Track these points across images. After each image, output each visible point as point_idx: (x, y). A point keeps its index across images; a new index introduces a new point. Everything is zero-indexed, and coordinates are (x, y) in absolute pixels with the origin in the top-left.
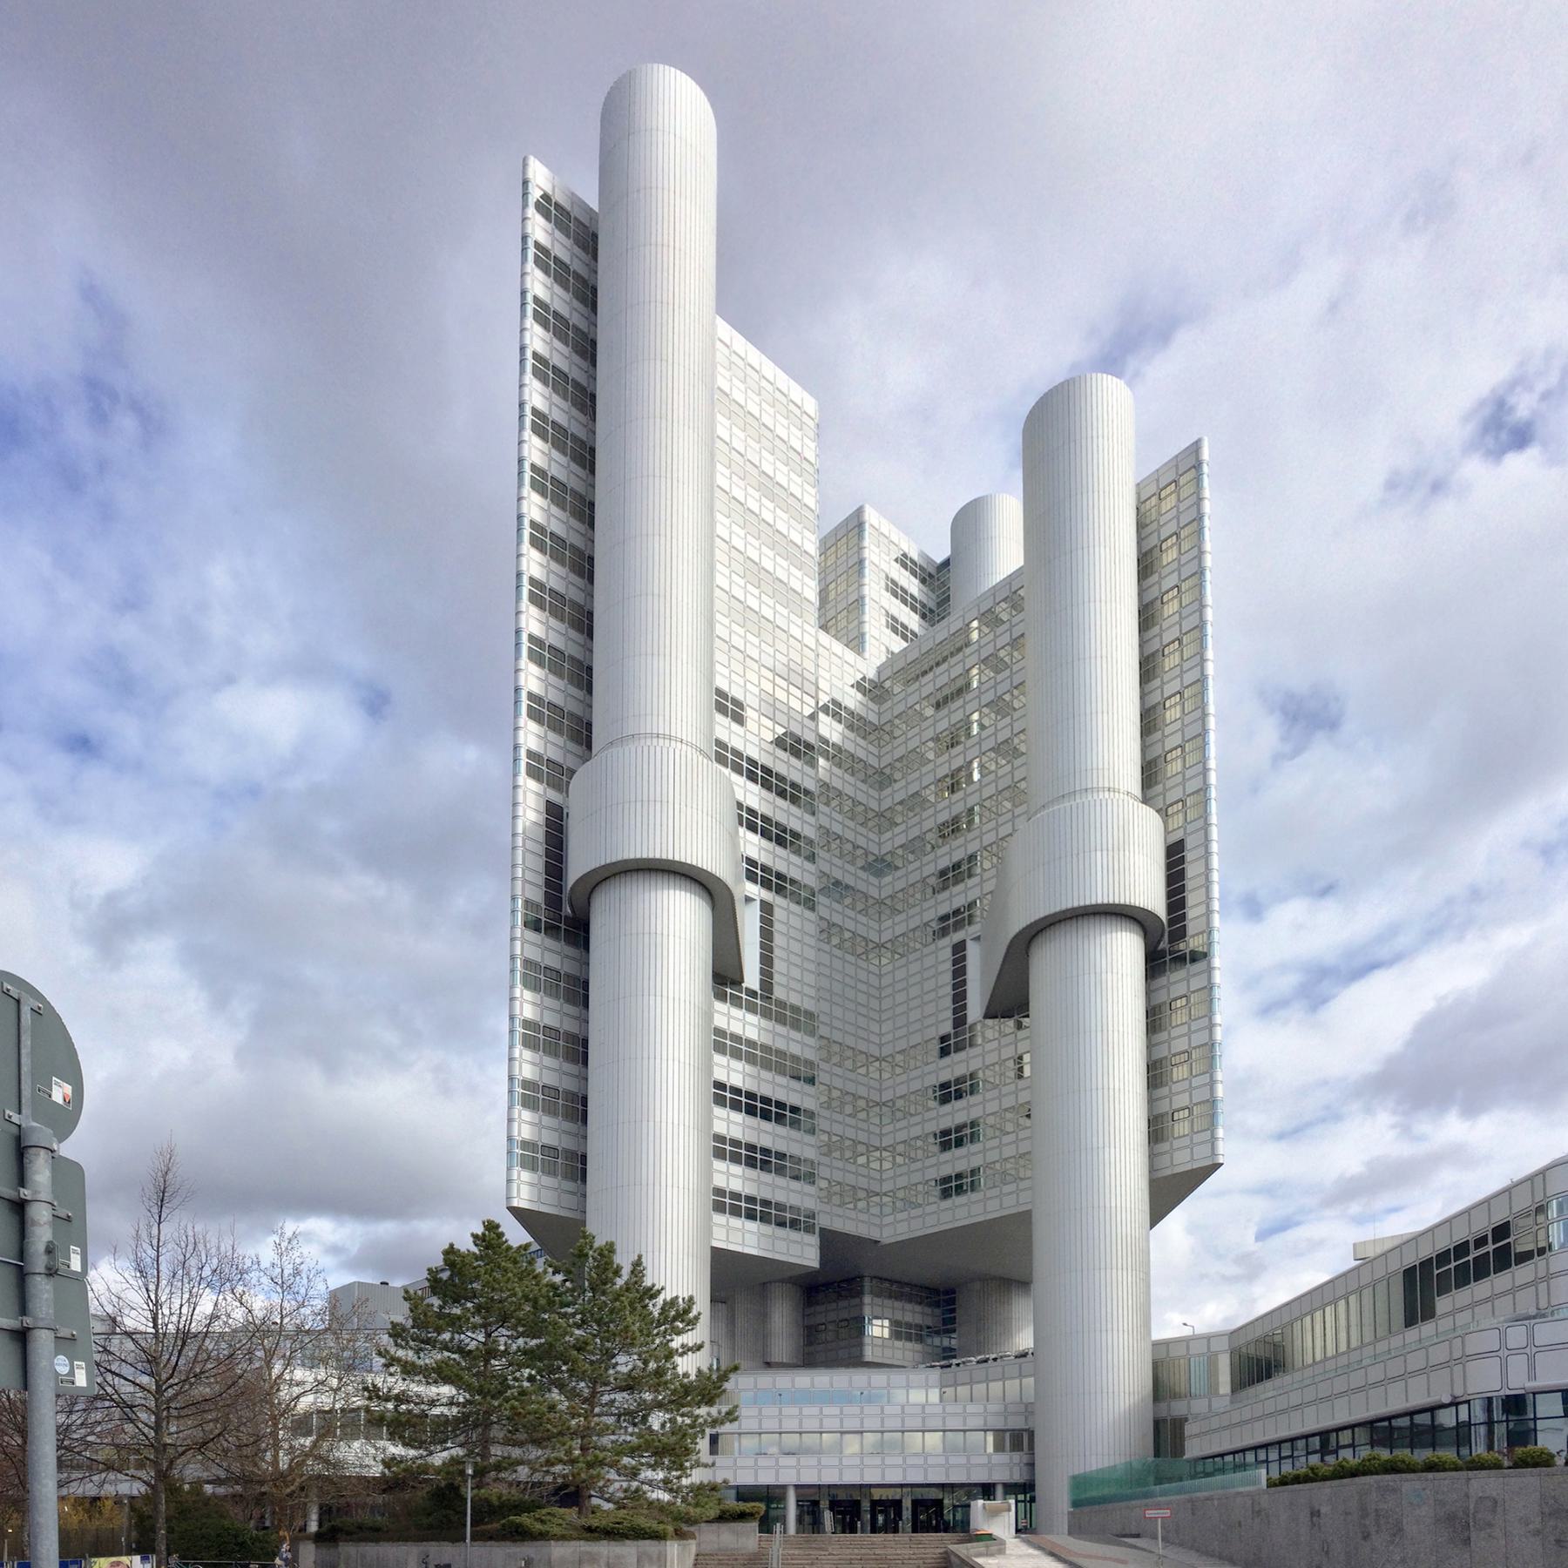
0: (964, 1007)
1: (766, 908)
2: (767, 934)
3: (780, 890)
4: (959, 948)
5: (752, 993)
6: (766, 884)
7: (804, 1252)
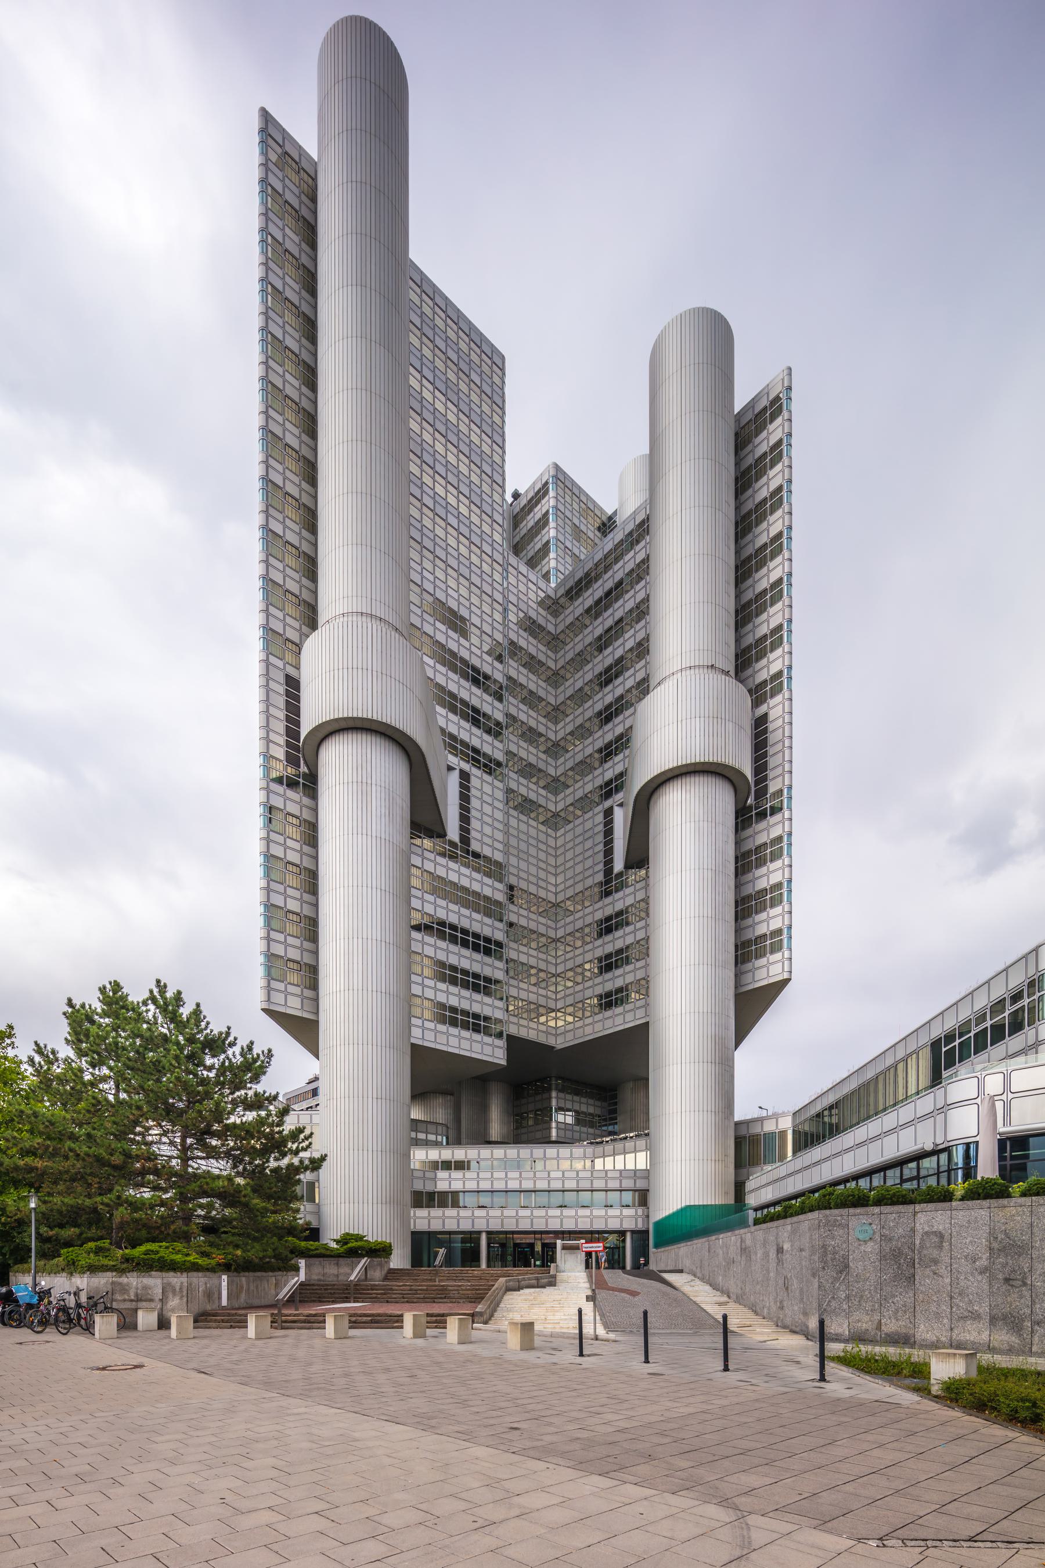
1: (465, 776)
2: (465, 798)
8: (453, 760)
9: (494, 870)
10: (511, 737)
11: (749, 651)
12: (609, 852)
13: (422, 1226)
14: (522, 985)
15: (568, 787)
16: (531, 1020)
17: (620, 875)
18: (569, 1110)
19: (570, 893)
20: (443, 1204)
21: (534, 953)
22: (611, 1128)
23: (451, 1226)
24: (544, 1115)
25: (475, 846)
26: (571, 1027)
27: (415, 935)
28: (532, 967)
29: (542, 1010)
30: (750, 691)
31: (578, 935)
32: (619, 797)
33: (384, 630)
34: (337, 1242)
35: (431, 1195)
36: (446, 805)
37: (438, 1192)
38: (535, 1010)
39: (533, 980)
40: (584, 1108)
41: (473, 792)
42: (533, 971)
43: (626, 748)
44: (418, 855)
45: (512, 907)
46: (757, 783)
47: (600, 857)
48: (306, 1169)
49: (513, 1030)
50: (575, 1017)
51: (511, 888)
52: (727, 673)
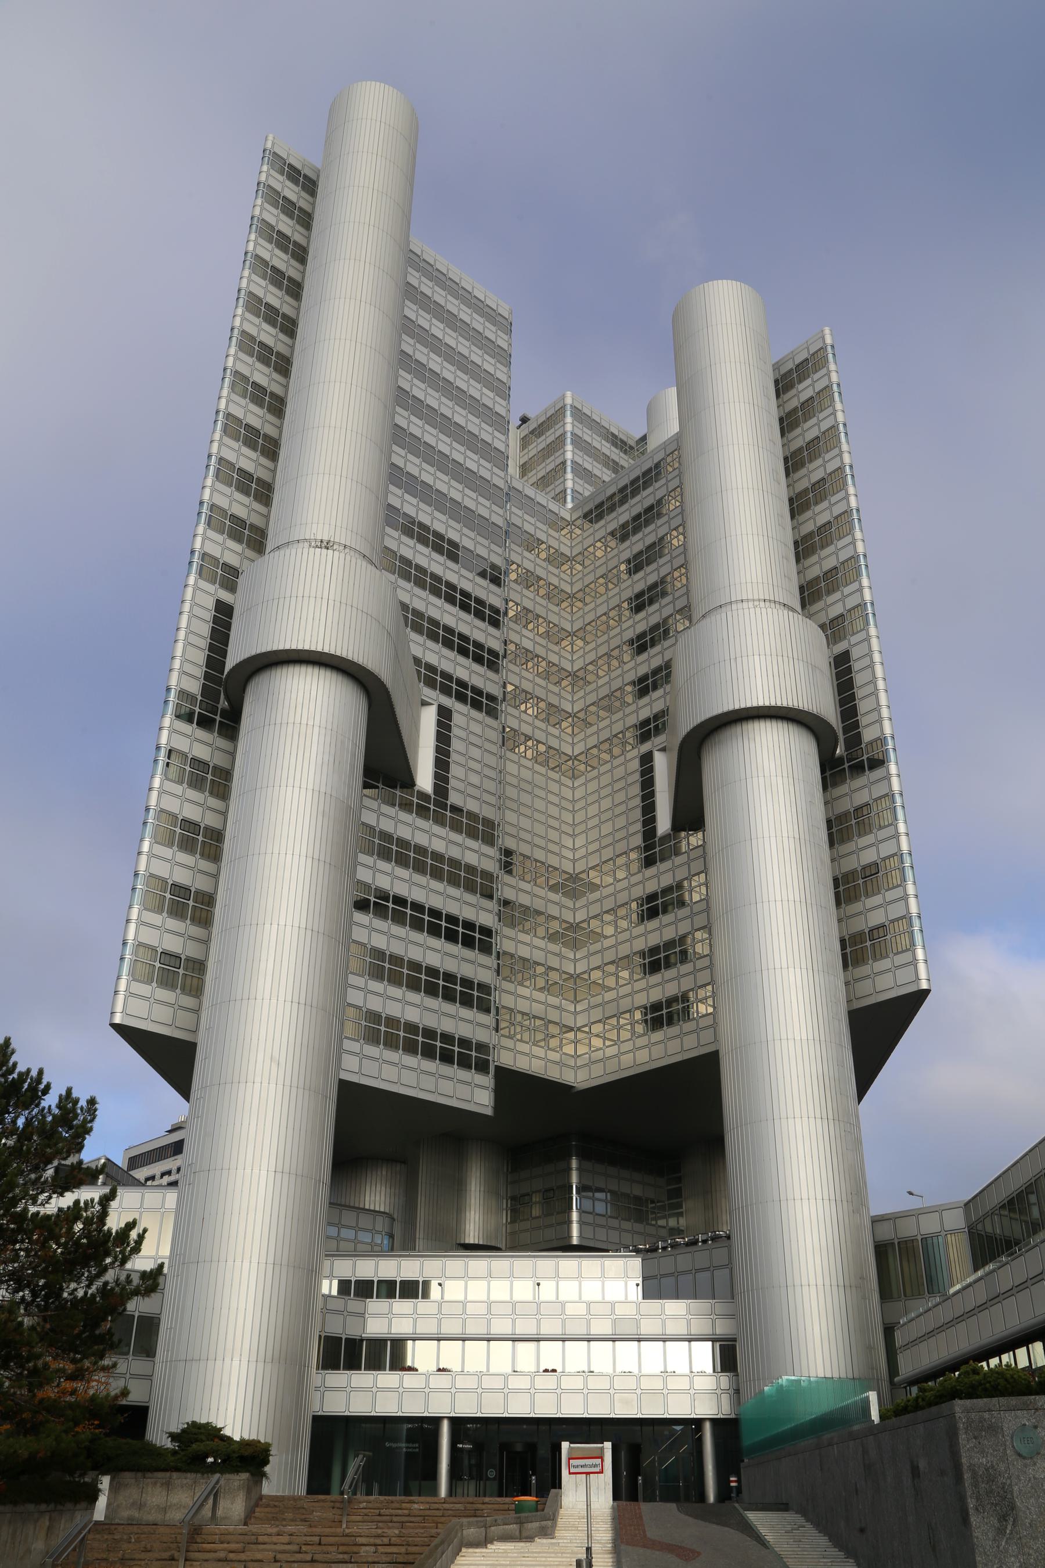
0: (653, 819)
1: (444, 714)
2: (443, 738)
3: (461, 698)
4: (647, 760)
5: (423, 796)
6: (446, 691)
7: (476, 1095)
8: (428, 693)
9: (482, 830)
10: (511, 667)
11: (819, 583)
12: (649, 808)
13: (336, 1405)
14: (521, 991)
15: (591, 725)
16: (536, 1043)
17: (666, 838)
18: (600, 1190)
19: (594, 860)
20: (375, 1364)
21: (541, 943)
22: (672, 1222)
23: (387, 1407)
24: (557, 1202)
25: (454, 798)
26: (599, 1055)
27: (360, 917)
28: (539, 964)
29: (553, 1029)
30: (822, 627)
31: (608, 918)
32: (659, 740)
33: (348, 557)
34: (173, 1437)
35: (354, 1345)
36: (416, 752)
37: (370, 1341)
38: (545, 1028)
39: (541, 982)
40: (625, 1188)
41: (455, 731)
42: (540, 970)
43: (668, 682)
45: (507, 879)
46: (846, 730)
47: (636, 790)
48: (136, 1292)
49: (505, 1059)
50: (605, 1039)
51: (508, 853)
52: (793, 610)
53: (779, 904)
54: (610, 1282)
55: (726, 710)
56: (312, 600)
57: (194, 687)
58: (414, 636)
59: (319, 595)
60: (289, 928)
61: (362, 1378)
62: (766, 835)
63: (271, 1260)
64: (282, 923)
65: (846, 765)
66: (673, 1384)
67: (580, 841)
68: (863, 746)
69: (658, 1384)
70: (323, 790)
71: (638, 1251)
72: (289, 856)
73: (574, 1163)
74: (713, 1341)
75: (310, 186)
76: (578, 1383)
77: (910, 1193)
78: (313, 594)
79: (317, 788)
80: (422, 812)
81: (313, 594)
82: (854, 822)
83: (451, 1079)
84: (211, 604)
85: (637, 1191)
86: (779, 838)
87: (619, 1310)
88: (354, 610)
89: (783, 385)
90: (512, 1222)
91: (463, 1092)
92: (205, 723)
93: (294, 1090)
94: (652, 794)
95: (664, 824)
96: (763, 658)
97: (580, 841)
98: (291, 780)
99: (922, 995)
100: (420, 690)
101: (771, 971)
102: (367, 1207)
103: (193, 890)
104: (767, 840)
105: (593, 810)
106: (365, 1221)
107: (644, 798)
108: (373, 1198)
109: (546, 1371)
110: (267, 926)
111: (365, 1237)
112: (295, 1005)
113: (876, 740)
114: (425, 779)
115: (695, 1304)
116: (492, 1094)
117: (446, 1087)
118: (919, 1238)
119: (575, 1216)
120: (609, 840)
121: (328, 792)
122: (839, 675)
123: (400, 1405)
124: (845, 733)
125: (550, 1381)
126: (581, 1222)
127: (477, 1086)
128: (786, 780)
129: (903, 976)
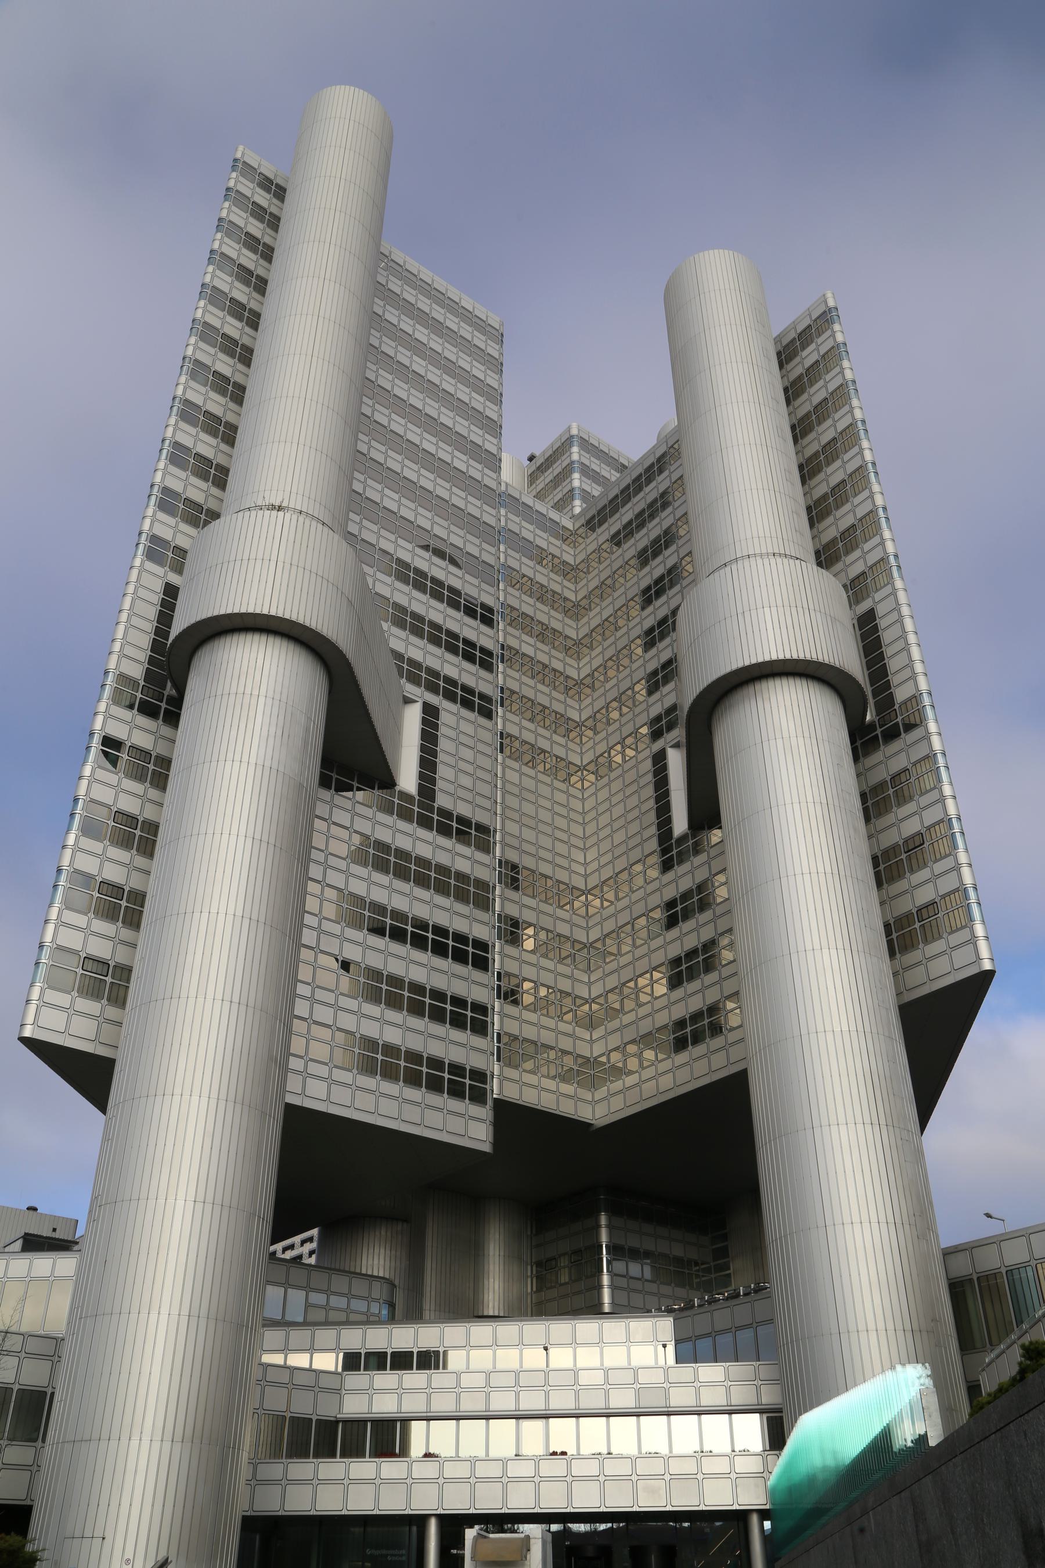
0: (669, 820)
1: (430, 713)
3: (450, 696)
4: (660, 759)
5: (405, 796)
6: (433, 688)
7: (470, 1128)
8: (411, 690)
25: (442, 801)
37: (345, 1422)
44: (346, 810)
53: (807, 877)
54: (635, 1346)
55: (734, 667)
56: (259, 562)
57: (137, 672)
58: (395, 630)
59: (267, 557)
60: (221, 916)
61: (332, 1468)
62: (788, 801)
63: (185, 1311)
64: (214, 910)
65: (879, 731)
66: (709, 1466)
67: (592, 854)
68: (897, 707)
69: (690, 1467)
70: (268, 764)
71: (669, 1311)
72: (225, 836)
73: (603, 1220)
74: (761, 1412)
75: (280, 193)
76: (592, 1468)
77: (988, 1216)
78: (260, 556)
79: (260, 762)
80: (405, 815)
81: (260, 556)
82: (891, 791)
83: (440, 1110)
84: (159, 586)
85: (678, 1251)
86: (803, 805)
87: (644, 1378)
88: (307, 573)
89: (785, 355)
90: (539, 1290)
91: (456, 1124)
92: (148, 710)
93: (222, 1104)
94: (667, 794)
95: (680, 824)
96: (774, 609)
97: (592, 854)
98: (230, 755)
99: (987, 977)
100: (401, 688)
101: (802, 954)
102: (364, 1271)
103: (127, 889)
104: (789, 807)
105: (604, 819)
106: (359, 1287)
107: (658, 800)
108: (370, 1262)
109: (554, 1453)
110: (197, 915)
111: (359, 1305)
112: (227, 1004)
113: (910, 699)
114: (408, 779)
115: (738, 1369)
116: (491, 1128)
117: (434, 1119)
118: (1003, 1270)
119: (606, 1279)
120: (623, 848)
121: (275, 766)
122: (863, 637)
123: (377, 1500)
124: (874, 696)
125: (557, 1468)
126: (613, 1287)
127: (472, 1118)
128: (808, 741)
129: (961, 957)
